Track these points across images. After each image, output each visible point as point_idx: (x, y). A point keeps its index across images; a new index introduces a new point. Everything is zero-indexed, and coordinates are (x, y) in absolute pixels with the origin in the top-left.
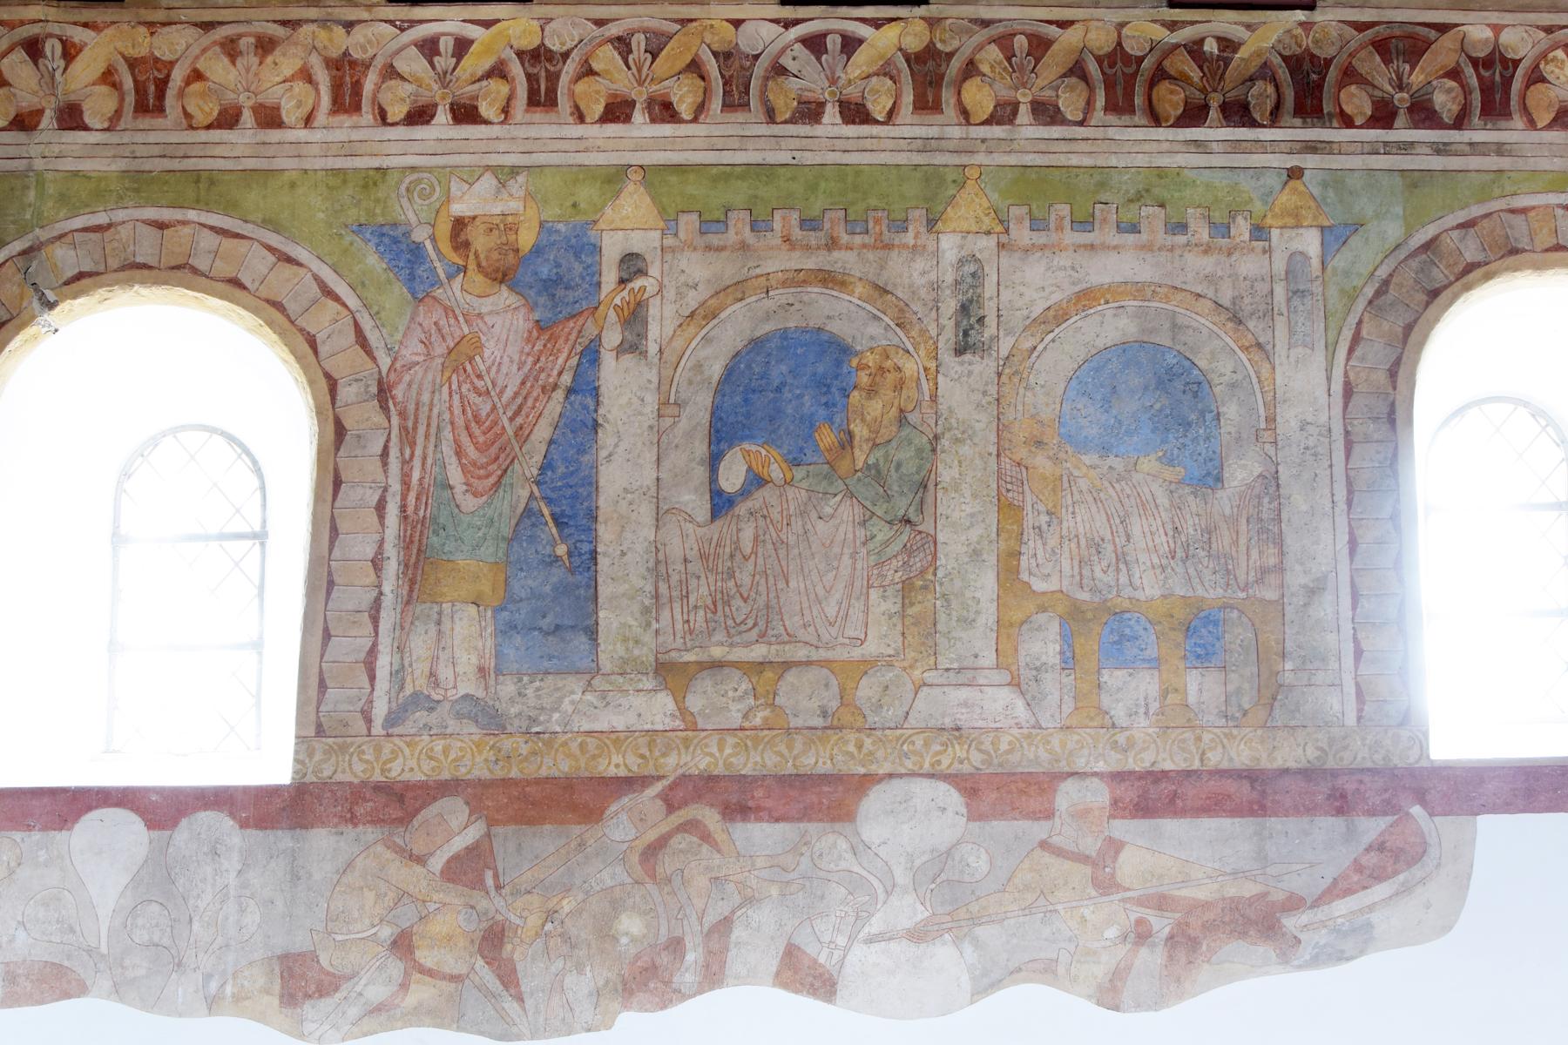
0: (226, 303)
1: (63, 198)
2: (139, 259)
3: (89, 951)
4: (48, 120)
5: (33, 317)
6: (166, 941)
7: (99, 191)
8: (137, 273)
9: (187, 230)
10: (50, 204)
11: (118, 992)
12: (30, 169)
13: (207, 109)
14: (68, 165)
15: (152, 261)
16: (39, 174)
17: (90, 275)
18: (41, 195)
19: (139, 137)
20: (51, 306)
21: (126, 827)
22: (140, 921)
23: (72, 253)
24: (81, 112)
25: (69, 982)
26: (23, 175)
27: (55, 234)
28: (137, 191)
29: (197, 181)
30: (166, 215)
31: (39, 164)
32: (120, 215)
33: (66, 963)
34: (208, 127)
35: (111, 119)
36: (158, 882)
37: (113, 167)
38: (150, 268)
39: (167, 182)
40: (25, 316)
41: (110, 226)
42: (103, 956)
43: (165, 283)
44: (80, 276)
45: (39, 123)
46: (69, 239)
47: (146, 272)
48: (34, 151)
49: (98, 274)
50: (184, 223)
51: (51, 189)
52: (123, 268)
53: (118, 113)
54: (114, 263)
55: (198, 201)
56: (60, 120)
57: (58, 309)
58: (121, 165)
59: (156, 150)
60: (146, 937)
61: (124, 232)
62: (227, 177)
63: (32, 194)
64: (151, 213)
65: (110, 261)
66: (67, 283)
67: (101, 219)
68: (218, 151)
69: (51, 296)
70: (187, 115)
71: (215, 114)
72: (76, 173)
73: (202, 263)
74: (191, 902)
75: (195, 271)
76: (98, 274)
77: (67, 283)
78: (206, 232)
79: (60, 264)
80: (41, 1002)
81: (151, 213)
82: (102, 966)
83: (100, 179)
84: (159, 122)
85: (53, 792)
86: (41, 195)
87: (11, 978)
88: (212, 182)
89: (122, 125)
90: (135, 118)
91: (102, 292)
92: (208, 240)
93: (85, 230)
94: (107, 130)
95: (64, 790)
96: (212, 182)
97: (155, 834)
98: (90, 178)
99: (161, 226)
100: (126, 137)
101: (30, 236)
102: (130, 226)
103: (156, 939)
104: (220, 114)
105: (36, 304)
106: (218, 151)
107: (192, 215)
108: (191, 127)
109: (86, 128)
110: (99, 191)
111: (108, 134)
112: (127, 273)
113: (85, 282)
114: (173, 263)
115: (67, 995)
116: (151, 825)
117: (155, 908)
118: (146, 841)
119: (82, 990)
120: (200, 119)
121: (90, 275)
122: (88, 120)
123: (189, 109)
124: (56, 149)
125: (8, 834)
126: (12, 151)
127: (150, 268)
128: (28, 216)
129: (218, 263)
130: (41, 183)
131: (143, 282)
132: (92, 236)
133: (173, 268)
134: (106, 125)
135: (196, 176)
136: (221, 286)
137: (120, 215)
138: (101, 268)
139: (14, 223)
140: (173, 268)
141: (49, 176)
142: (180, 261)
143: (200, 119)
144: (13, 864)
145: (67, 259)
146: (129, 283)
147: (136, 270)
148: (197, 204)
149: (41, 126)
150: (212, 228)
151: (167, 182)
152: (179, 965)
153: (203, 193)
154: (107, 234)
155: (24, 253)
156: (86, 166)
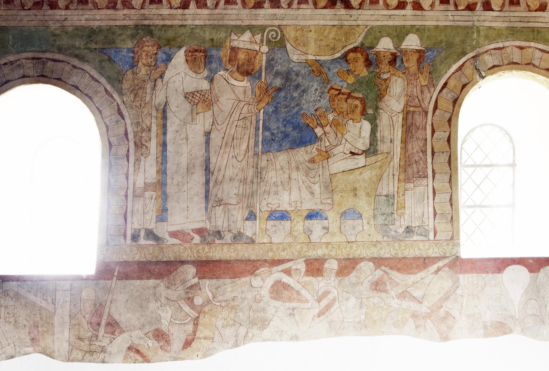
0: (545, 78)
1: (487, 37)
2: (515, 61)
3: (512, 317)
4: (479, 7)
5: (478, 82)
6: (538, 313)
7: (499, 34)
8: (514, 66)
9: (530, 50)
10: (482, 39)
11: (523, 331)
12: (474, 25)
13: (535, 4)
14: (487, 24)
15: (519, 62)
16: (478, 28)
17: (497, 66)
18: (479, 35)
19: (512, 14)
20: (483, 78)
21: (521, 271)
22: (529, 306)
23: (491, 58)
24: (491, 4)
25: (506, 328)
26: (472, 27)
27: (485, 50)
28: (512, 34)
29: (533, 31)
30: (523, 44)
31: (477, 24)
32: (507, 44)
33: (504, 322)
34: (536, 11)
35: (501, 7)
36: (534, 292)
37: (504, 25)
38: (519, 64)
39: (522, 32)
40: (474, 81)
41: (504, 48)
42: (517, 319)
43: (524, 70)
44: (494, 67)
45: (476, 8)
46: (489, 52)
47: (517, 66)
48: (475, 18)
49: (500, 66)
50: (530, 47)
51: (482, 33)
52: (509, 64)
53: (503, 5)
54: (506, 62)
55: (534, 39)
56: (484, 7)
57: (485, 79)
58: (506, 25)
59: (518, 19)
60: (531, 312)
61: (509, 50)
62: (544, 30)
63: (475, 35)
64: (518, 43)
65: (504, 61)
66: (489, 69)
67: (500, 45)
68: (540, 20)
69: (484, 74)
70: (528, 6)
71: (538, 5)
72: (490, 28)
73: (537, 63)
74: (546, 299)
75: (534, 65)
76: (500, 66)
77: (489, 69)
78: (537, 51)
79: (487, 62)
80: (497, 336)
81: (518, 43)
82: (517, 323)
83: (499, 30)
84: (518, 8)
85: (495, 260)
86: (479, 35)
87: (485, 327)
88: (538, 32)
89: (505, 9)
90: (509, 7)
91: (501, 73)
92: (538, 54)
93: (495, 49)
94: (500, 11)
95: (499, 259)
96: (538, 32)
97: (532, 274)
98: (495, 29)
99: (521, 48)
100: (507, 14)
101: (476, 51)
102: (510, 48)
103: (535, 313)
104: (540, 5)
105: (478, 77)
106: (540, 20)
107: (532, 44)
108: (530, 11)
109: (492, 10)
110: (499, 34)
111: (500, 13)
112: (511, 66)
113: (496, 69)
114: (526, 63)
115: (505, 333)
116: (531, 271)
117: (534, 301)
118: (529, 277)
119: (511, 331)
120: (533, 7)
121: (497, 66)
122: (493, 7)
123: (529, 4)
124: (483, 18)
125: (480, 275)
126: (467, 18)
127: (519, 64)
128: (474, 44)
129: (542, 63)
130: (478, 31)
131: (516, 69)
132: (497, 51)
133: (527, 64)
134: (500, 9)
135: (533, 29)
136: (543, 71)
137: (507, 44)
138: (501, 64)
139: (469, 46)
140: (527, 64)
141: (481, 28)
142: (529, 62)
143: (533, 7)
144: (483, 286)
145: (489, 60)
146: (511, 69)
147: (513, 65)
148: (534, 40)
149: (477, 9)
150: (539, 49)
151: (522, 32)
152: (543, 322)
153: (535, 36)
154: (503, 51)
155: (473, 57)
156: (494, 24)
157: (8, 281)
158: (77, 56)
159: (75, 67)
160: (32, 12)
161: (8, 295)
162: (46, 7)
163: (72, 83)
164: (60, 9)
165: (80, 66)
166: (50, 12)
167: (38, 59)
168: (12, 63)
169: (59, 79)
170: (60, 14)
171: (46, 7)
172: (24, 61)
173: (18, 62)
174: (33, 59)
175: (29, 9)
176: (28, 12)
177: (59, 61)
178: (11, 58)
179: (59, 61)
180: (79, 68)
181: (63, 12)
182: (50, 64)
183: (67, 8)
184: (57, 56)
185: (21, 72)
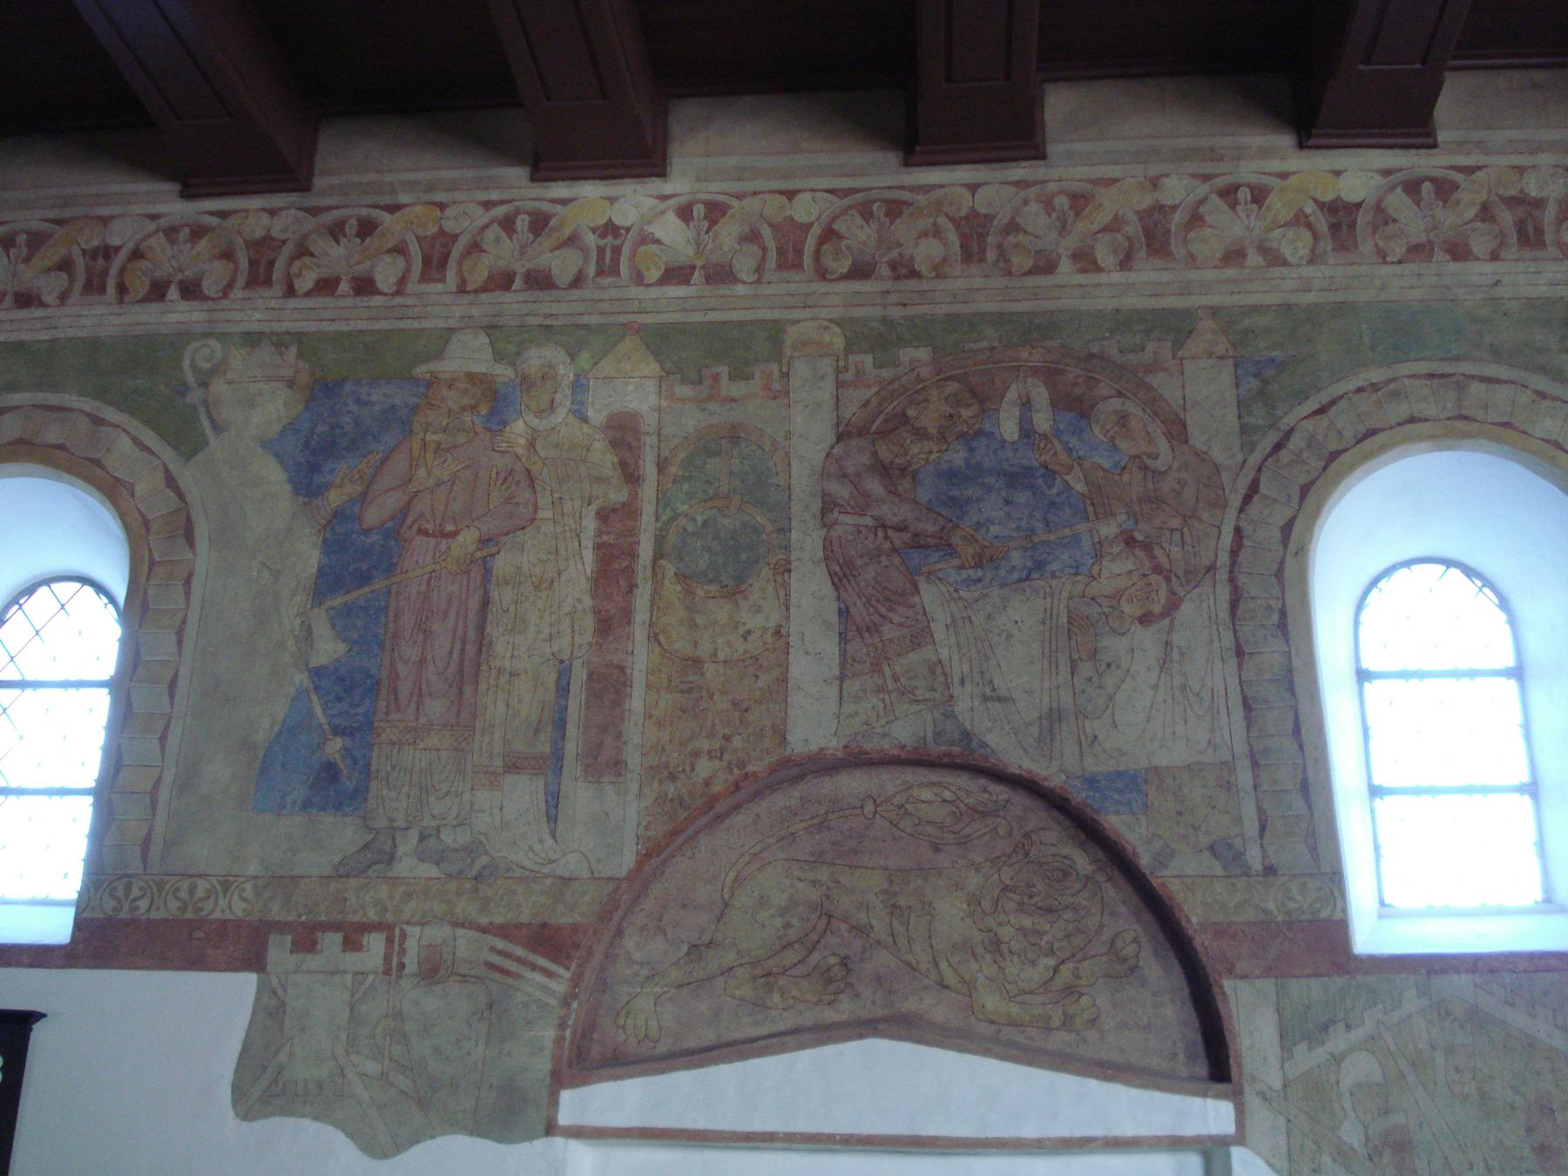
157: (1443, 971)
158: (1543, 369)
159: (1542, 395)
160: (1407, 268)
161: (1448, 1014)
162: (1439, 255)
163: (1542, 435)
164: (1478, 259)
165: (1556, 392)
166: (1454, 267)
167: (1442, 376)
168: (1375, 387)
169: (1506, 425)
170: (1480, 271)
171: (1439, 255)
172: (1407, 382)
173: (1393, 386)
174: (1431, 376)
175: (1400, 262)
176: (1398, 269)
177: (1498, 381)
178: (1376, 375)
179: (1498, 381)
180: (1555, 398)
181: (1488, 267)
182: (1476, 388)
183: (1494, 256)
184: (1491, 370)
185: (1401, 410)
